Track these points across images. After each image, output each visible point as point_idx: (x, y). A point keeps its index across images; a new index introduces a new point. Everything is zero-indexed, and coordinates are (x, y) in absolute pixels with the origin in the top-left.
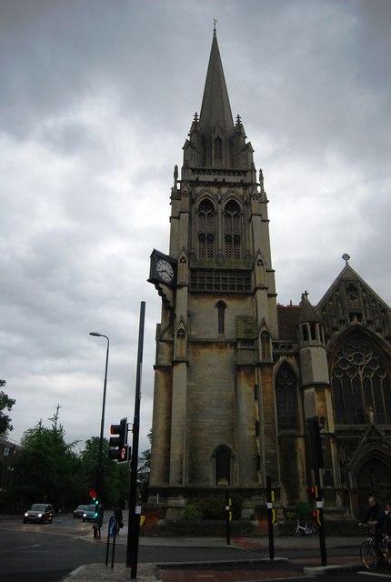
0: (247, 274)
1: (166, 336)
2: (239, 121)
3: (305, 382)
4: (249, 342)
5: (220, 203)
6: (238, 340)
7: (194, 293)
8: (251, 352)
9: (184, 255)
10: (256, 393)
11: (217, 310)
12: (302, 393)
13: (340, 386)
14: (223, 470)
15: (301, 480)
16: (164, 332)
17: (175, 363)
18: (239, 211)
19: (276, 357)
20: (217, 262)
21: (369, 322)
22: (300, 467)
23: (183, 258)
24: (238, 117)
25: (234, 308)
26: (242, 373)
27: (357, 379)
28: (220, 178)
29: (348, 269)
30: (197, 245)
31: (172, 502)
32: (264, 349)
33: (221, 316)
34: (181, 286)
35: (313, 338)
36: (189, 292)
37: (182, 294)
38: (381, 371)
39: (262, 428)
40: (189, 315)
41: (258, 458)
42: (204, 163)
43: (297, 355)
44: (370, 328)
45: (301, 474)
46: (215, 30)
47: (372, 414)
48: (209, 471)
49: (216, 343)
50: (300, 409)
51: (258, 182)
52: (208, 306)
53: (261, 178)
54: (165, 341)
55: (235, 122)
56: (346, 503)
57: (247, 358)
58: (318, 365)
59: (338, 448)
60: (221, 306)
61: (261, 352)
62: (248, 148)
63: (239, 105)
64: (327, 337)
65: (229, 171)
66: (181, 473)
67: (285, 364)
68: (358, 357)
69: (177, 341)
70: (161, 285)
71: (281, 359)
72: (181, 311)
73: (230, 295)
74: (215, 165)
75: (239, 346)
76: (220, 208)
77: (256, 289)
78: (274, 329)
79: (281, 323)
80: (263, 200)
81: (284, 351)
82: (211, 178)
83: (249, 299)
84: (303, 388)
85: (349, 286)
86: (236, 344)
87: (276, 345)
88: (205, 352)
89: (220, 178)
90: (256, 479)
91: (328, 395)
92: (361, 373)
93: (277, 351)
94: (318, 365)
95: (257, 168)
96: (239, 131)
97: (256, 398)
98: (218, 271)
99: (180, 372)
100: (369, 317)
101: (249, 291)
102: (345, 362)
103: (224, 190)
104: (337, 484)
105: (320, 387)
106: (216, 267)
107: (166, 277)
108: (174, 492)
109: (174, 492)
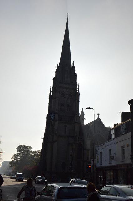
2: (73, 64)
24: (73, 62)
29: (98, 118)
36: (58, 122)
37: (57, 123)
46: (67, 19)
53: (79, 87)
55: (72, 65)
60: (66, 126)
62: (76, 75)
71: (79, 141)
95: (78, 84)
96: (73, 68)
103: (68, 90)
107: (52, 117)
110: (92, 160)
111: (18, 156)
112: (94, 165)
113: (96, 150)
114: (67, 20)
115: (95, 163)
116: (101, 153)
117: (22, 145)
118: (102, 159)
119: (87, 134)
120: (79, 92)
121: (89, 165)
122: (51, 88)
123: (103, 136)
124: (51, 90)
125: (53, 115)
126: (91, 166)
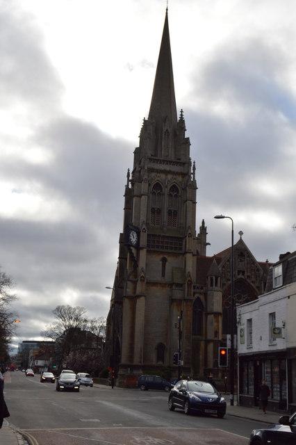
0: (181, 239)
1: (131, 277)
2: (182, 115)
3: (209, 310)
4: (180, 285)
5: (166, 187)
9: (144, 226)
11: (161, 262)
12: (207, 317)
14: (160, 357)
16: (130, 275)
17: (139, 296)
19: (194, 293)
21: (248, 276)
22: (201, 356)
23: (144, 229)
24: (182, 112)
25: (172, 262)
26: (175, 304)
28: (168, 168)
29: (241, 241)
32: (188, 291)
33: (164, 266)
34: (142, 248)
36: (147, 251)
37: (143, 253)
40: (146, 265)
43: (205, 295)
44: (248, 281)
46: (167, 10)
48: (153, 356)
49: (160, 284)
51: (192, 171)
52: (157, 259)
53: (194, 169)
55: (178, 119)
57: (178, 294)
60: (164, 260)
64: (224, 284)
67: (198, 298)
69: (139, 283)
70: (132, 248)
71: (196, 295)
72: (142, 264)
73: (169, 254)
76: (166, 191)
77: (186, 253)
78: (194, 277)
80: (194, 187)
81: (198, 291)
83: (181, 256)
84: (207, 314)
89: (168, 169)
91: (220, 319)
93: (195, 291)
95: (192, 162)
99: (141, 303)
101: (181, 252)
103: (170, 177)
105: (216, 314)
106: (162, 234)
107: (133, 238)
110: (229, 336)
112: (233, 350)
113: (238, 314)
114: (167, 13)
115: (235, 343)
116: (250, 321)
118: (253, 335)
120: (195, 181)
121: (221, 350)
122: (128, 173)
124: (130, 178)
125: (135, 235)
126: (225, 350)
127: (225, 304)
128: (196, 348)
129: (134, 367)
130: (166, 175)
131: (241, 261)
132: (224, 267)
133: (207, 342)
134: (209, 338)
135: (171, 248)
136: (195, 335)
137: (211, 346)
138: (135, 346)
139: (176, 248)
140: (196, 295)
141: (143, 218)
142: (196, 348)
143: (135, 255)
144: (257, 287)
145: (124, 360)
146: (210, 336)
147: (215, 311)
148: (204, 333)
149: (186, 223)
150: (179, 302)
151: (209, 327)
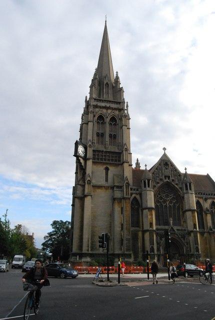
1: (81, 182)
2: (117, 75)
3: (144, 206)
6: (115, 186)
7: (94, 163)
8: (120, 192)
9: (90, 143)
10: (122, 211)
11: (105, 171)
13: (159, 209)
15: (140, 250)
16: (80, 180)
17: (86, 196)
18: (116, 122)
19: (131, 195)
20: (105, 148)
22: (139, 244)
24: (117, 73)
25: (112, 170)
26: (116, 201)
27: (166, 206)
29: (165, 155)
30: (95, 136)
31: (84, 260)
32: (126, 191)
34: (89, 159)
35: (148, 187)
36: (93, 162)
37: (90, 163)
38: (177, 202)
39: (125, 227)
41: (122, 240)
42: (99, 95)
43: (141, 195)
45: (140, 248)
47: (172, 222)
50: (141, 218)
51: (126, 108)
52: (101, 169)
53: (127, 106)
54: (80, 185)
55: (115, 75)
56: (158, 260)
57: (118, 194)
58: (150, 199)
59: (157, 236)
60: (107, 169)
61: (125, 192)
62: (121, 89)
63: (119, 65)
65: (112, 102)
66: (88, 247)
67: (135, 197)
68: (167, 196)
69: (87, 186)
71: (133, 195)
73: (111, 164)
74: (105, 97)
75: (115, 189)
76: (108, 120)
77: (124, 162)
78: (131, 182)
79: (134, 178)
80: (127, 117)
81: (135, 192)
82: (103, 104)
85: (165, 163)
86: (114, 189)
87: (131, 189)
88: (99, 191)
89: (108, 105)
90: (121, 249)
92: (168, 203)
93: (132, 192)
94: (150, 199)
95: (126, 102)
97: (122, 213)
98: (106, 152)
99: (88, 201)
100: (173, 178)
101: (119, 163)
102: (161, 198)
103: (109, 111)
104: (156, 252)
105: (150, 209)
108: (86, 255)
109: (86, 255)
111: (55, 234)
117: (59, 220)
119: (147, 183)
123: (176, 184)
127: (156, 202)
128: (135, 237)
129: (82, 255)
130: (107, 110)
131: (167, 169)
132: (153, 173)
133: (144, 232)
134: (145, 228)
135: (112, 160)
136: (133, 227)
137: (147, 235)
138: (84, 237)
139: (116, 161)
140: (133, 195)
141: (90, 137)
142: (135, 237)
143: (83, 164)
144: (181, 188)
145: (75, 249)
146: (147, 227)
147: (149, 206)
148: (141, 225)
149: (123, 142)
150: (120, 200)
151: (145, 220)
